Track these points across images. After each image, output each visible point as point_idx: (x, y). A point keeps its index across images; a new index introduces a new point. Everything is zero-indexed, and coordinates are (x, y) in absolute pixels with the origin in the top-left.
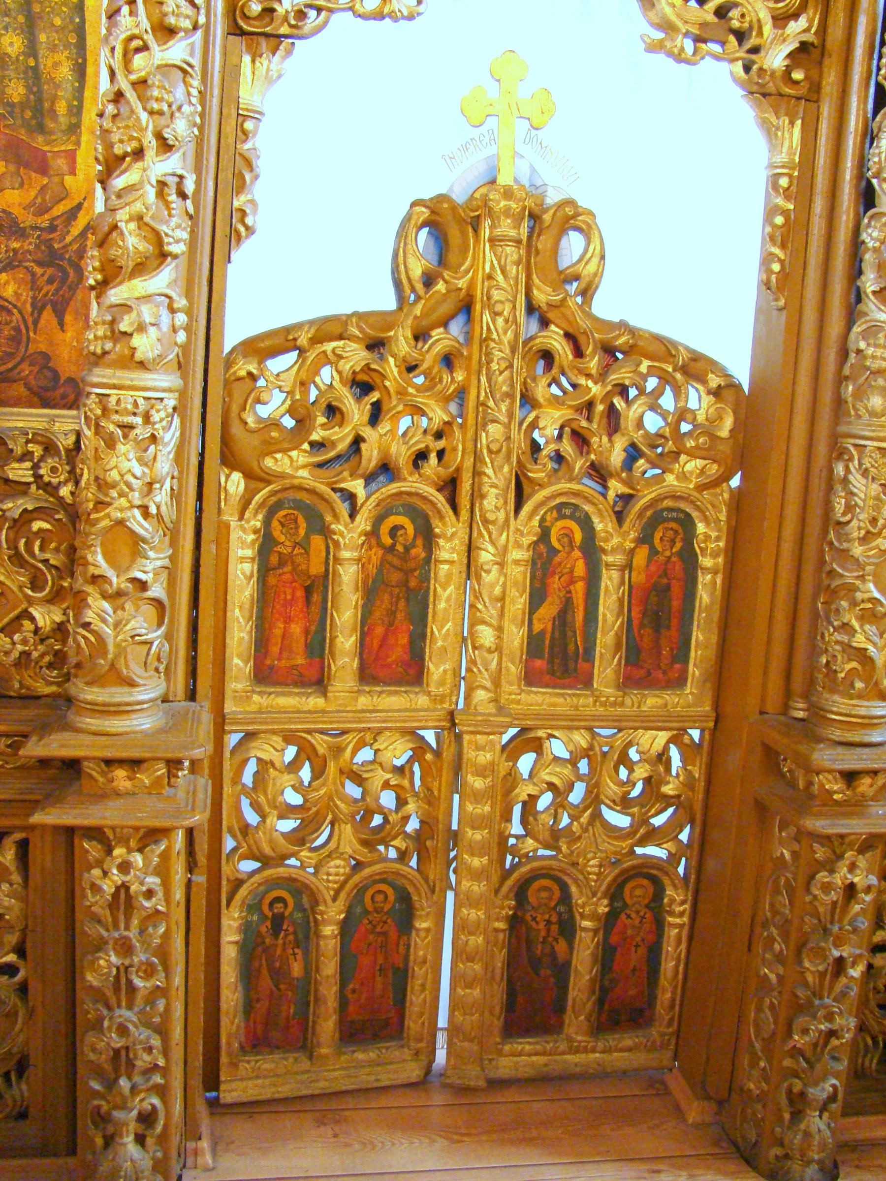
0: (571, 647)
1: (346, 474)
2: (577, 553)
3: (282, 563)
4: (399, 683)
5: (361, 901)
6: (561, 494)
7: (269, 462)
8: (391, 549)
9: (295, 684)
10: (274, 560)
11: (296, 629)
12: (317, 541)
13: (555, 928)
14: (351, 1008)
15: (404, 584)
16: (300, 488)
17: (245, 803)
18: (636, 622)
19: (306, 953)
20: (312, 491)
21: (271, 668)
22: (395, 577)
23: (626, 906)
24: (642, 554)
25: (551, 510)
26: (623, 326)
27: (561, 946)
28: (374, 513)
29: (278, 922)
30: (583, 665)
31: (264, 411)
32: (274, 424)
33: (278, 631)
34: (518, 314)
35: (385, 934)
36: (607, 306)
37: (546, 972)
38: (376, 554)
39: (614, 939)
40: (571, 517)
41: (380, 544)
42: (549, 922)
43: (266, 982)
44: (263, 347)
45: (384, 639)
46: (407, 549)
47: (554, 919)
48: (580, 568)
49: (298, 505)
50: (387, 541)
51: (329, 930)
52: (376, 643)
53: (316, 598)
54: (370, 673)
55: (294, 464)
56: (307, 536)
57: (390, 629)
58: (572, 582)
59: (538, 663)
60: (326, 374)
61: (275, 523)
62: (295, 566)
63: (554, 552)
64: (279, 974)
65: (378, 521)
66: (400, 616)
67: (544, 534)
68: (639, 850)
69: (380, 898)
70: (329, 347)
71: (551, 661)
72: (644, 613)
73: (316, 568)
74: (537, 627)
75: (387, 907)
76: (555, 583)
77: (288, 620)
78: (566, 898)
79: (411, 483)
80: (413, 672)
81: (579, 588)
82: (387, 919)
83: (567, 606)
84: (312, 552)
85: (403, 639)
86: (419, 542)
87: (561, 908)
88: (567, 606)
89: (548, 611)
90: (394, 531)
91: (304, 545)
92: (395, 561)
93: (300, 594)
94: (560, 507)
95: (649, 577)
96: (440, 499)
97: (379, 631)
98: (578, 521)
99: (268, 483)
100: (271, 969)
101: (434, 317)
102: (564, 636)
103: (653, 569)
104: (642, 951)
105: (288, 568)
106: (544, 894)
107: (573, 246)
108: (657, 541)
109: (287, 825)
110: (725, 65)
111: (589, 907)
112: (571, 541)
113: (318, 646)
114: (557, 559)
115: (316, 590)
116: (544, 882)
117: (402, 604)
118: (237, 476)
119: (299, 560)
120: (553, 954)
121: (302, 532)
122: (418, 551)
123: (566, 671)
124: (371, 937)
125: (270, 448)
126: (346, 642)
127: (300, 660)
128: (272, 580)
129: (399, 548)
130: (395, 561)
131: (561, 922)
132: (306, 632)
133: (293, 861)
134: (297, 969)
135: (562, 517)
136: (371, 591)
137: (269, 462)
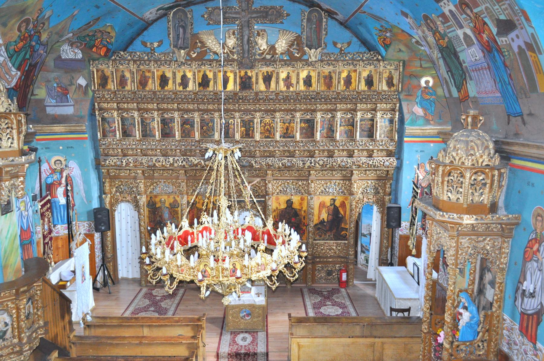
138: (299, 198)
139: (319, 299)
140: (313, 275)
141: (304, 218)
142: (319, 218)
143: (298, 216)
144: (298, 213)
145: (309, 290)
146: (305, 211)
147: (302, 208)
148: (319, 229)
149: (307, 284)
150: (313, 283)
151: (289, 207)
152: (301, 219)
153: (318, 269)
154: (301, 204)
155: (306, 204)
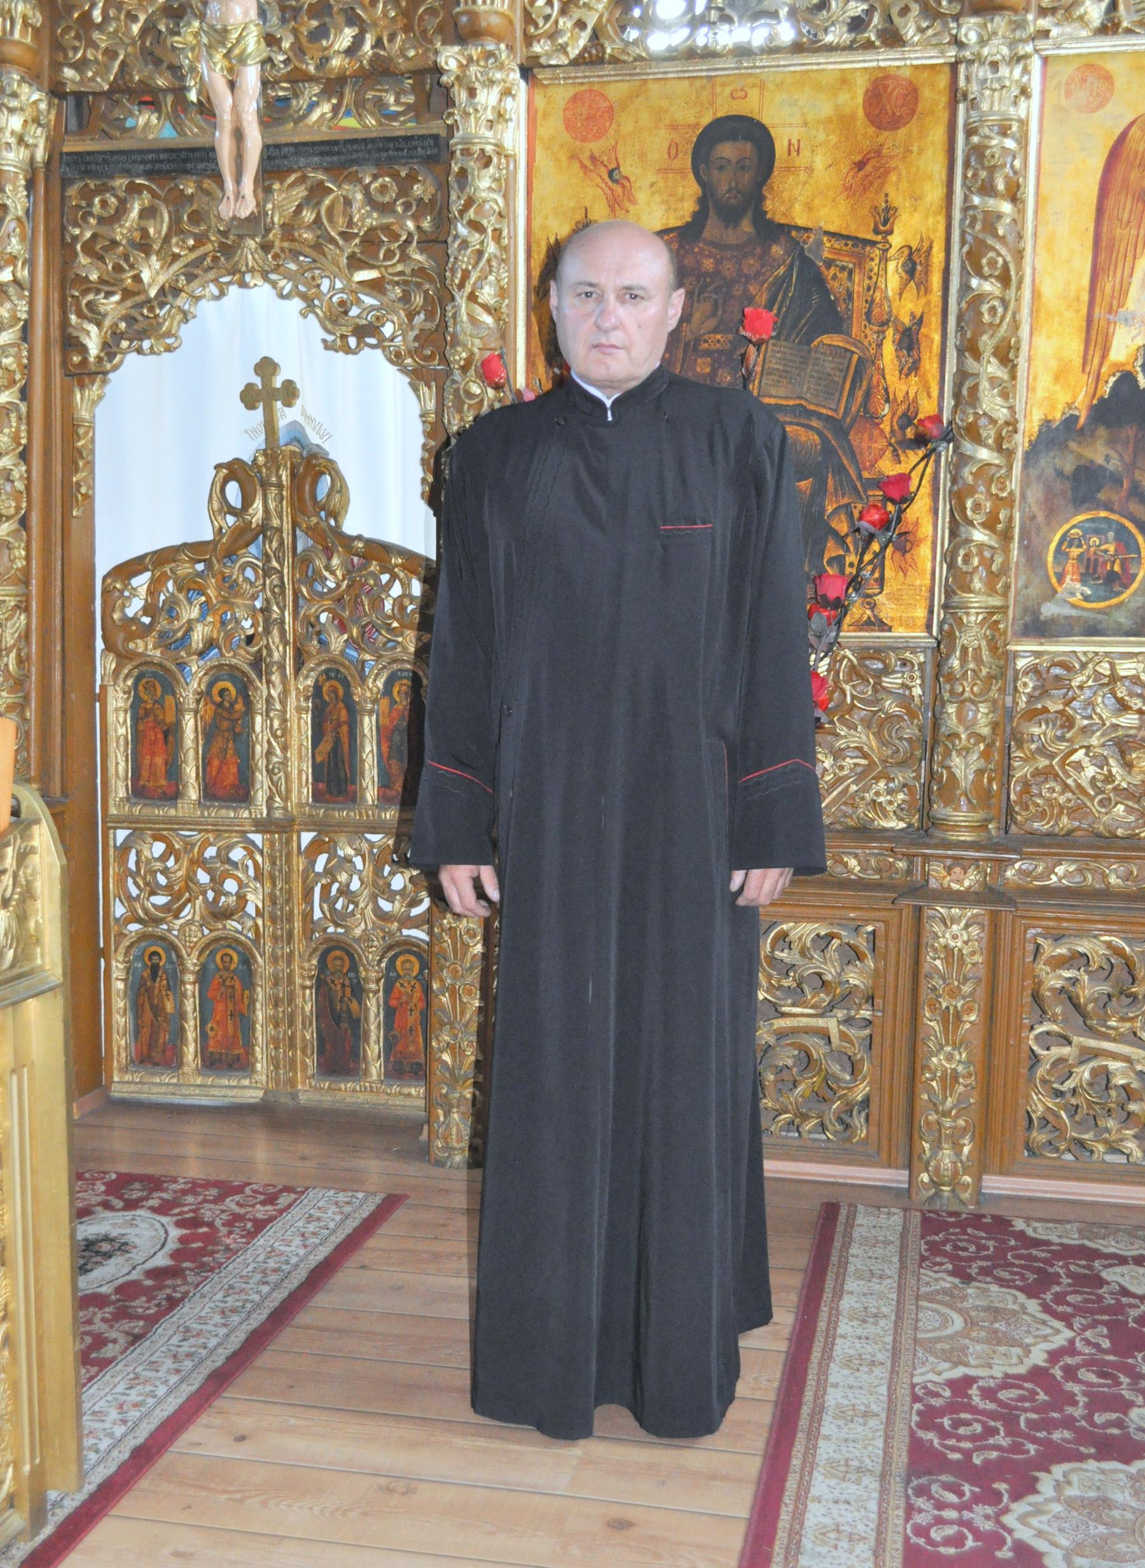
0: (342, 774)
1: (183, 653)
2: (341, 705)
3: (147, 713)
4: (234, 801)
5: (214, 961)
6: (324, 661)
7: (131, 645)
8: (220, 705)
9: (160, 799)
10: (142, 712)
11: (159, 761)
12: (169, 699)
13: (348, 990)
14: (211, 1042)
15: (232, 730)
16: (152, 663)
17: (130, 880)
18: (385, 755)
19: (175, 994)
20: (160, 665)
21: (143, 787)
22: (225, 724)
23: (399, 976)
24: (385, 702)
25: (321, 673)
26: (359, 538)
27: (354, 1006)
28: (206, 679)
29: (155, 970)
30: (351, 788)
31: (130, 612)
32: (135, 620)
33: (147, 761)
34: (285, 535)
35: (233, 987)
36: (350, 526)
37: (344, 1025)
38: (211, 708)
39: (394, 1003)
40: (336, 678)
41: (213, 702)
42: (343, 985)
43: (148, 1014)
44: (126, 570)
45: (220, 769)
46: (232, 705)
47: (347, 983)
48: (344, 715)
49: (155, 675)
50: (218, 699)
51: (190, 978)
52: (214, 771)
53: (171, 738)
54: (211, 792)
55: (147, 647)
56: (162, 696)
57: (224, 762)
58: (339, 725)
59: (321, 785)
60: (170, 585)
61: (140, 688)
62: (156, 716)
63: (326, 704)
64: (158, 1010)
65: (210, 685)
66: (230, 752)
67: (317, 688)
68: (405, 932)
69: (227, 959)
70: (167, 569)
71: (329, 784)
72: (390, 747)
73: (170, 718)
74: (319, 759)
75: (233, 967)
76: (329, 726)
77: (153, 754)
78: (354, 967)
79: (229, 658)
80: (242, 794)
81: (344, 729)
82: (230, 976)
83: (337, 742)
84: (167, 706)
85: (234, 770)
86: (240, 700)
87: (351, 975)
88: (337, 742)
89: (326, 746)
90: (222, 692)
91: (160, 702)
92: (225, 714)
93: (160, 736)
94: (327, 671)
95: (392, 721)
96: (246, 668)
97: (216, 763)
98: (339, 680)
99: (131, 659)
100: (151, 1004)
101: (241, 542)
102: (336, 765)
103: (394, 715)
104: (416, 1014)
105: (151, 719)
106: (338, 963)
107: (326, 481)
108: (395, 693)
109: (161, 900)
110: (379, 352)
111: (372, 973)
112: (337, 696)
113: (174, 772)
114: (328, 709)
115: (172, 732)
116: (338, 953)
117: (231, 745)
118: (111, 656)
119: (158, 712)
120: (349, 1011)
121: (159, 693)
122: (239, 706)
123: (340, 792)
124: (223, 989)
125: (131, 637)
126: (191, 771)
127: (163, 782)
128: (141, 727)
129: (227, 704)
130: (225, 714)
131: (351, 985)
132: (166, 763)
133: (165, 927)
134: (169, 1006)
135: (329, 678)
136: (209, 734)
137: (131, 645)
138: (854, 99)
139: (1038, 1337)
140: (1000, 1065)
141: (909, 340)
142: (1095, 336)
143: (836, 322)
144: (837, 285)
145: (931, 1224)
146: (914, 265)
147: (885, 219)
148: (1085, 485)
149: (911, 1162)
150: (982, 1166)
151: (730, 217)
152: (864, 367)
153: (1066, 993)
154: (867, 170)
155: (933, 163)
